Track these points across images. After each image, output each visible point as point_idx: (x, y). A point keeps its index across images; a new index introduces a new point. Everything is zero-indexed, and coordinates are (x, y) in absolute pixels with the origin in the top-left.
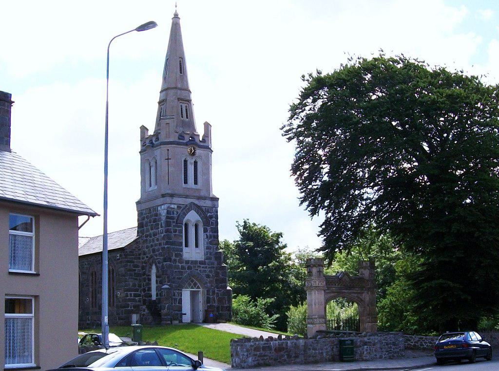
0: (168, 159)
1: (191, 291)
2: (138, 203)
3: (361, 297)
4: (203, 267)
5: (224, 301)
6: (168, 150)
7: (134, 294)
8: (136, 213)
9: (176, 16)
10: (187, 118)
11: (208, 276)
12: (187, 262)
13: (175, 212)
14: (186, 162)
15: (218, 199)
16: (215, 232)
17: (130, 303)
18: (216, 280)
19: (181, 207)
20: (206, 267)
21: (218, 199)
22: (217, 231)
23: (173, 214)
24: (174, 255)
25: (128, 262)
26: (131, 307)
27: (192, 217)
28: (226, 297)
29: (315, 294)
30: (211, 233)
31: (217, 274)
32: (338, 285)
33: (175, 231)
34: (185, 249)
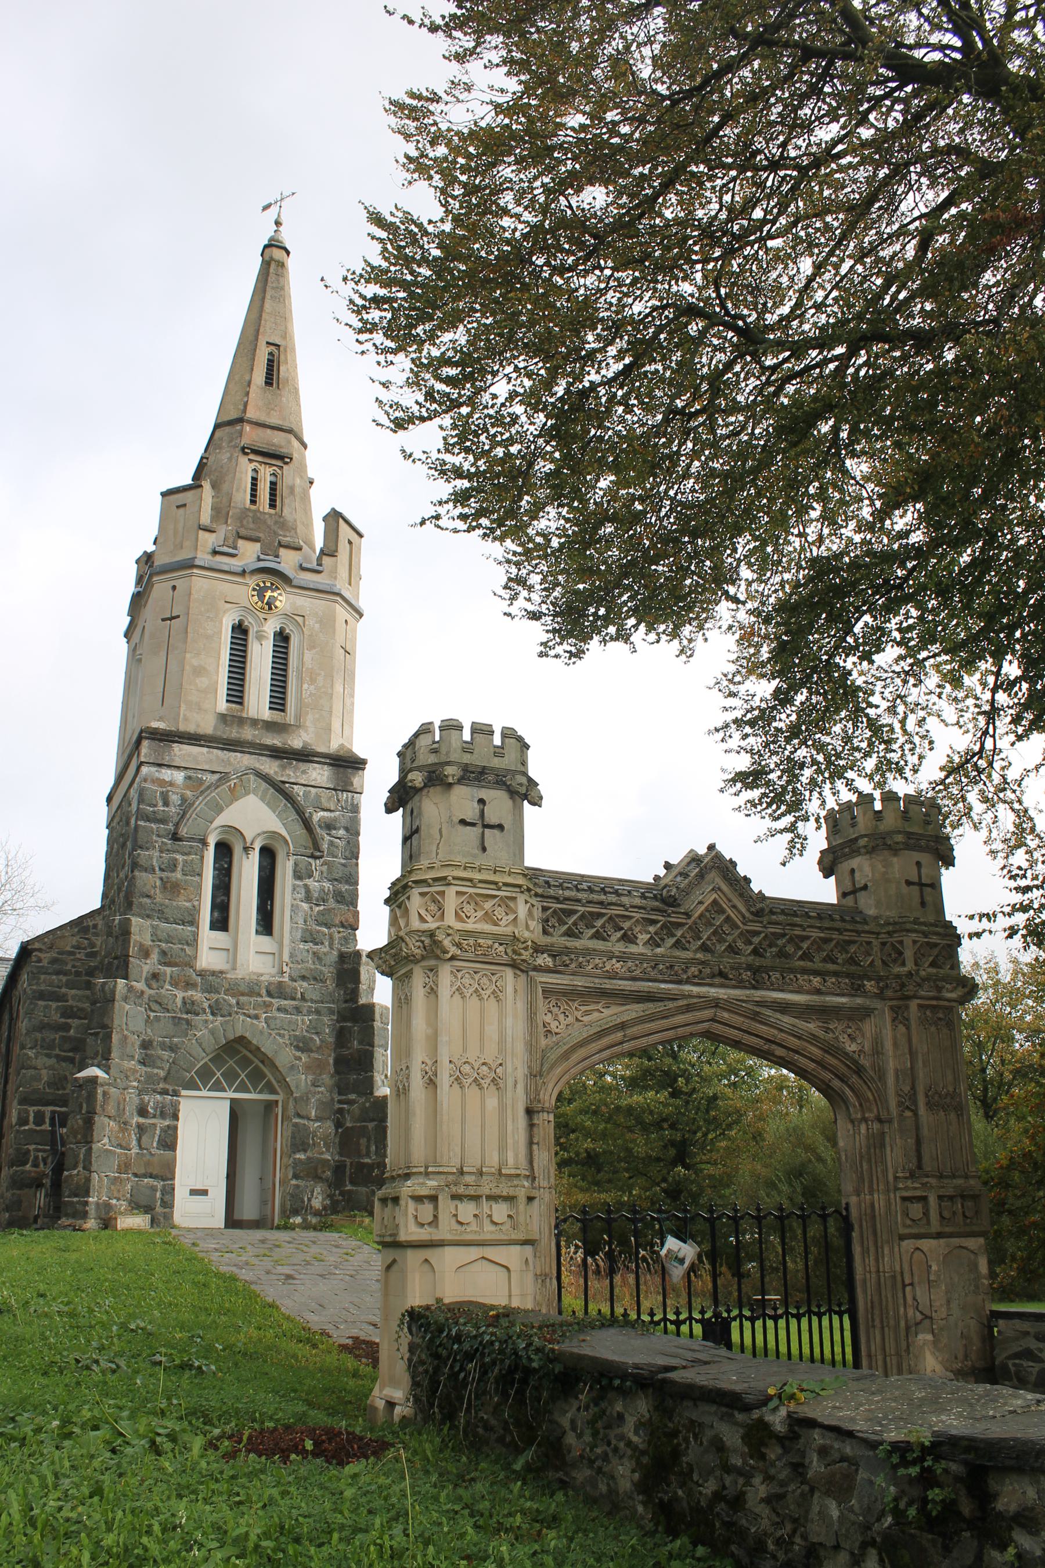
0: (171, 619)
1: (232, 1100)
2: (109, 799)
3: (852, 1047)
4: (279, 1009)
5: (363, 1141)
6: (174, 588)
7: (53, 1112)
8: (103, 834)
9: (274, 245)
10: (273, 505)
11: (302, 1045)
12: (211, 980)
13: (175, 798)
14: (240, 631)
15: (364, 762)
16: (347, 882)
17: (32, 1147)
18: (337, 1062)
19: (201, 782)
20: (298, 1010)
21: (364, 762)
22: (352, 879)
23: (166, 804)
24: (155, 956)
25: (41, 996)
26: (35, 1165)
27: (253, 816)
28: (371, 1125)
29: (433, 991)
30: (327, 885)
31: (341, 1037)
32: (653, 943)
33: (173, 866)
34: (208, 937)
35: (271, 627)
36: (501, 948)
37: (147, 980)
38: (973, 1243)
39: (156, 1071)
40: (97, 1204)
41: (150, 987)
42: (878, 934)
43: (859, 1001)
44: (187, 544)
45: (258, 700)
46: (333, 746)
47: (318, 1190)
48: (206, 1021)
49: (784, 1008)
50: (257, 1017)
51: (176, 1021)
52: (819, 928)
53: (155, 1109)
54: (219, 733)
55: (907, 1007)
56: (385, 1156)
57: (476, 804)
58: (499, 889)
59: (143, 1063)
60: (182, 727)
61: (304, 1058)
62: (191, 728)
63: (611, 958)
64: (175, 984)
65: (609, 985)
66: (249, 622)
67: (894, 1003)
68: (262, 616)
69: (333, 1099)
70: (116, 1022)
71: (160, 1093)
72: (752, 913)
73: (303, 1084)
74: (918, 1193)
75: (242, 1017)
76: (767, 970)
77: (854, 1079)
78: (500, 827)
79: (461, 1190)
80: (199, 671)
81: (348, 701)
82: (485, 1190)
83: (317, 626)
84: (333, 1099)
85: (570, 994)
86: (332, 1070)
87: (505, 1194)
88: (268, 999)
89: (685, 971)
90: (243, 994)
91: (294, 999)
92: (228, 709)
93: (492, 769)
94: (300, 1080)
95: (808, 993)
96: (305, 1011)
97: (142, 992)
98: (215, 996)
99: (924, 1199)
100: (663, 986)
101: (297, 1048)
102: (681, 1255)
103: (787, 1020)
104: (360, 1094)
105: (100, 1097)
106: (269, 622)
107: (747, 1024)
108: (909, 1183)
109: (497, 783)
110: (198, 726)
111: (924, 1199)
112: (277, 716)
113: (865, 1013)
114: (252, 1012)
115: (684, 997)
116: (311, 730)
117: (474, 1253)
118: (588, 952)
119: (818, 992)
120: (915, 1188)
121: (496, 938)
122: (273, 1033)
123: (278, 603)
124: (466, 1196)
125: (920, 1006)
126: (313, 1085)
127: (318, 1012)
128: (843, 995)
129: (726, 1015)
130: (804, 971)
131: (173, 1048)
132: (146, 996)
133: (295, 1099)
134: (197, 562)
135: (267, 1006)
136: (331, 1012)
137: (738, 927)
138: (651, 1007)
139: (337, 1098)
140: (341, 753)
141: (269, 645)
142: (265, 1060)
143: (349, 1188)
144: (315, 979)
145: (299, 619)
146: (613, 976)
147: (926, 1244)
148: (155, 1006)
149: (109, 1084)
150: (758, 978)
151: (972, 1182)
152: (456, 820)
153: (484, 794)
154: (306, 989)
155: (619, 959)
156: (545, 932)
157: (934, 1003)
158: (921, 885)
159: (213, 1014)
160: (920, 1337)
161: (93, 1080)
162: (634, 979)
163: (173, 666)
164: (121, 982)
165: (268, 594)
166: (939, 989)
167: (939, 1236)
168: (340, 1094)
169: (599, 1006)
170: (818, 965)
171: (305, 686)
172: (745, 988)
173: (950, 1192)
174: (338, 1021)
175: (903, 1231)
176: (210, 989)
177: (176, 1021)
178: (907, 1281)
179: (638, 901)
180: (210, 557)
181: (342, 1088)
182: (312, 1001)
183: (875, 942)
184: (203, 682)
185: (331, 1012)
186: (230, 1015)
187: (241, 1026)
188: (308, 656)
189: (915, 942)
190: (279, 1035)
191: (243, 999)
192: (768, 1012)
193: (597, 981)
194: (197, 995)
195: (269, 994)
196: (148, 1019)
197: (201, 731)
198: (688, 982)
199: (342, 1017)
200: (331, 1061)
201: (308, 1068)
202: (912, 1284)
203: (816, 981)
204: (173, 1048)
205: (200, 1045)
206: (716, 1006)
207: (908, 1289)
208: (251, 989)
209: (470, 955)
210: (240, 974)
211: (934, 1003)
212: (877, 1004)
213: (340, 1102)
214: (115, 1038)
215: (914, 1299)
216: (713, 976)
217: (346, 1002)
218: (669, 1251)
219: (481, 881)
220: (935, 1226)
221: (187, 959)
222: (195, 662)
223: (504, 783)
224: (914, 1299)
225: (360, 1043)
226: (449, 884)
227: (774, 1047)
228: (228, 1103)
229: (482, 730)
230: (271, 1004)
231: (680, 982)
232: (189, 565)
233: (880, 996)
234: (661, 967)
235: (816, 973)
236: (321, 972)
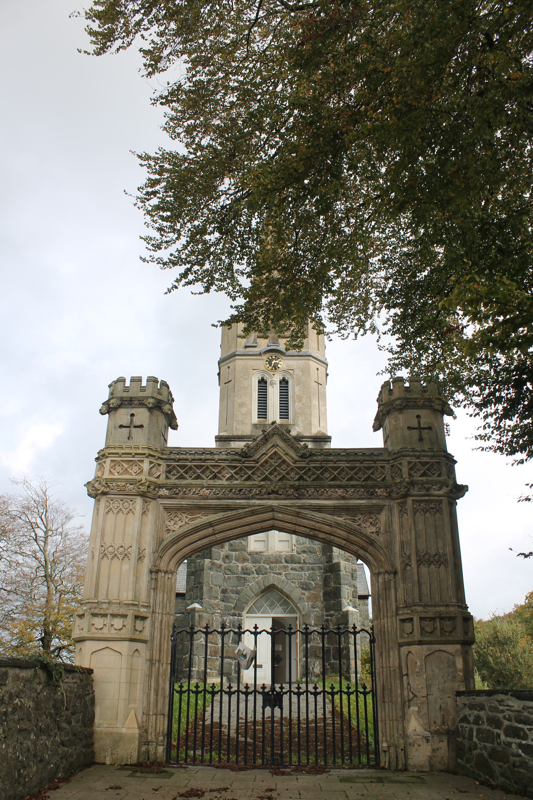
4: (292, 569)
11: (305, 587)
14: (262, 382)
18: (325, 594)
20: (302, 569)
21: (330, 438)
31: (326, 581)
35: (277, 378)
36: (131, 486)
37: (223, 559)
38: (450, 648)
39: (229, 604)
40: (198, 672)
41: (225, 562)
42: (389, 461)
43: (374, 501)
44: (233, 345)
45: (274, 414)
46: (314, 431)
47: (317, 663)
48: (254, 578)
49: (319, 509)
50: (280, 574)
51: (239, 578)
52: (346, 461)
53: (230, 623)
54: (253, 434)
55: (406, 502)
56: (349, 643)
57: (129, 417)
58: (134, 457)
59: (222, 600)
60: (235, 434)
61: (307, 593)
62: (240, 433)
63: (203, 488)
64: (237, 560)
65: (202, 502)
66: (266, 377)
67: (399, 501)
68: (271, 373)
69: (323, 615)
70: (205, 580)
71: (232, 615)
72: (299, 457)
73: (307, 607)
74: (408, 616)
75: (272, 575)
76: (305, 487)
77: (370, 548)
78: (141, 426)
79: (96, 611)
80: (242, 405)
81: (322, 408)
82: (110, 612)
83: (301, 373)
84: (323, 615)
85: (181, 509)
86: (322, 599)
87: (120, 613)
88: (286, 564)
89: (250, 492)
90: (272, 563)
91: (300, 563)
92: (258, 421)
93: (135, 398)
94: (306, 605)
95: (336, 499)
96: (306, 569)
97: (221, 565)
98: (258, 565)
99: (411, 620)
100: (238, 501)
101: (303, 588)
102: (244, 653)
103: (318, 516)
104: (336, 611)
105: (197, 617)
106: (276, 376)
107: (294, 519)
108: (406, 611)
109: (140, 404)
110: (243, 431)
111: (411, 620)
112: (284, 421)
113: (379, 509)
114: (278, 571)
115: (250, 506)
116: (301, 425)
117: (103, 644)
118: (187, 486)
119: (343, 498)
120: (408, 614)
121: (127, 481)
122: (288, 581)
123: (279, 366)
124: (100, 614)
125: (413, 500)
126: (312, 607)
127: (313, 569)
128: (362, 499)
129: (280, 515)
130: (330, 487)
131: (237, 592)
132: (223, 567)
133: (303, 615)
134: (237, 353)
135: (285, 568)
136: (320, 568)
137: (291, 466)
138: (229, 513)
139: (325, 613)
140: (318, 435)
141: (277, 387)
142: (288, 597)
143: (333, 661)
144: (310, 552)
145: (291, 372)
146: (206, 498)
147: (414, 648)
148: (228, 572)
149: (203, 611)
150: (299, 492)
151: (452, 609)
152: (118, 425)
153: (133, 411)
154: (306, 557)
155: (208, 488)
156: (167, 478)
157: (426, 498)
158: (420, 428)
159: (257, 574)
160: (411, 709)
161: (194, 610)
162: (219, 499)
163: (230, 405)
164: (207, 561)
165: (273, 362)
166: (428, 489)
167: (420, 643)
168: (326, 611)
169: (200, 515)
170: (344, 482)
171: (296, 404)
172: (292, 499)
173: (430, 615)
174: (324, 573)
175: (401, 641)
176: (255, 561)
177: (239, 578)
178: (404, 673)
179: (224, 457)
180: (244, 350)
181: (327, 608)
182: (309, 563)
183: (387, 466)
184: (244, 410)
185: (320, 568)
186: (266, 574)
187: (272, 579)
188: (297, 389)
189: (409, 463)
190: (293, 582)
191: (272, 565)
192: (307, 512)
193: (196, 501)
194: (249, 565)
195: (286, 561)
196: (224, 579)
197: (244, 434)
198: (253, 498)
199: (326, 571)
200: (321, 594)
201: (309, 598)
202: (407, 675)
203: (340, 492)
204: (237, 592)
205: (251, 590)
206: (273, 511)
207: (405, 677)
208: (276, 560)
209: (115, 492)
210: (270, 552)
211: (426, 498)
212: (387, 502)
213: (327, 616)
214: (205, 588)
215: (408, 684)
216: (269, 494)
217: (327, 562)
218: (239, 650)
219: (123, 454)
220: (417, 636)
221: (243, 547)
222: (239, 401)
223: (144, 404)
224: (408, 684)
225: (334, 583)
226: (107, 457)
227: (316, 532)
228: (271, 620)
229: (136, 380)
230: (287, 567)
231: (248, 498)
232: (234, 355)
233: (389, 496)
234: (234, 490)
235: (339, 487)
236: (313, 548)
